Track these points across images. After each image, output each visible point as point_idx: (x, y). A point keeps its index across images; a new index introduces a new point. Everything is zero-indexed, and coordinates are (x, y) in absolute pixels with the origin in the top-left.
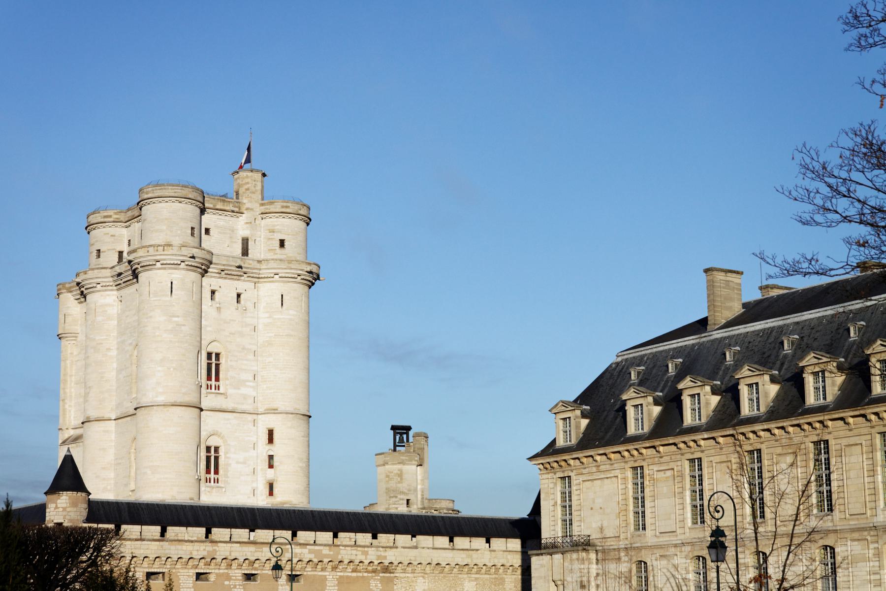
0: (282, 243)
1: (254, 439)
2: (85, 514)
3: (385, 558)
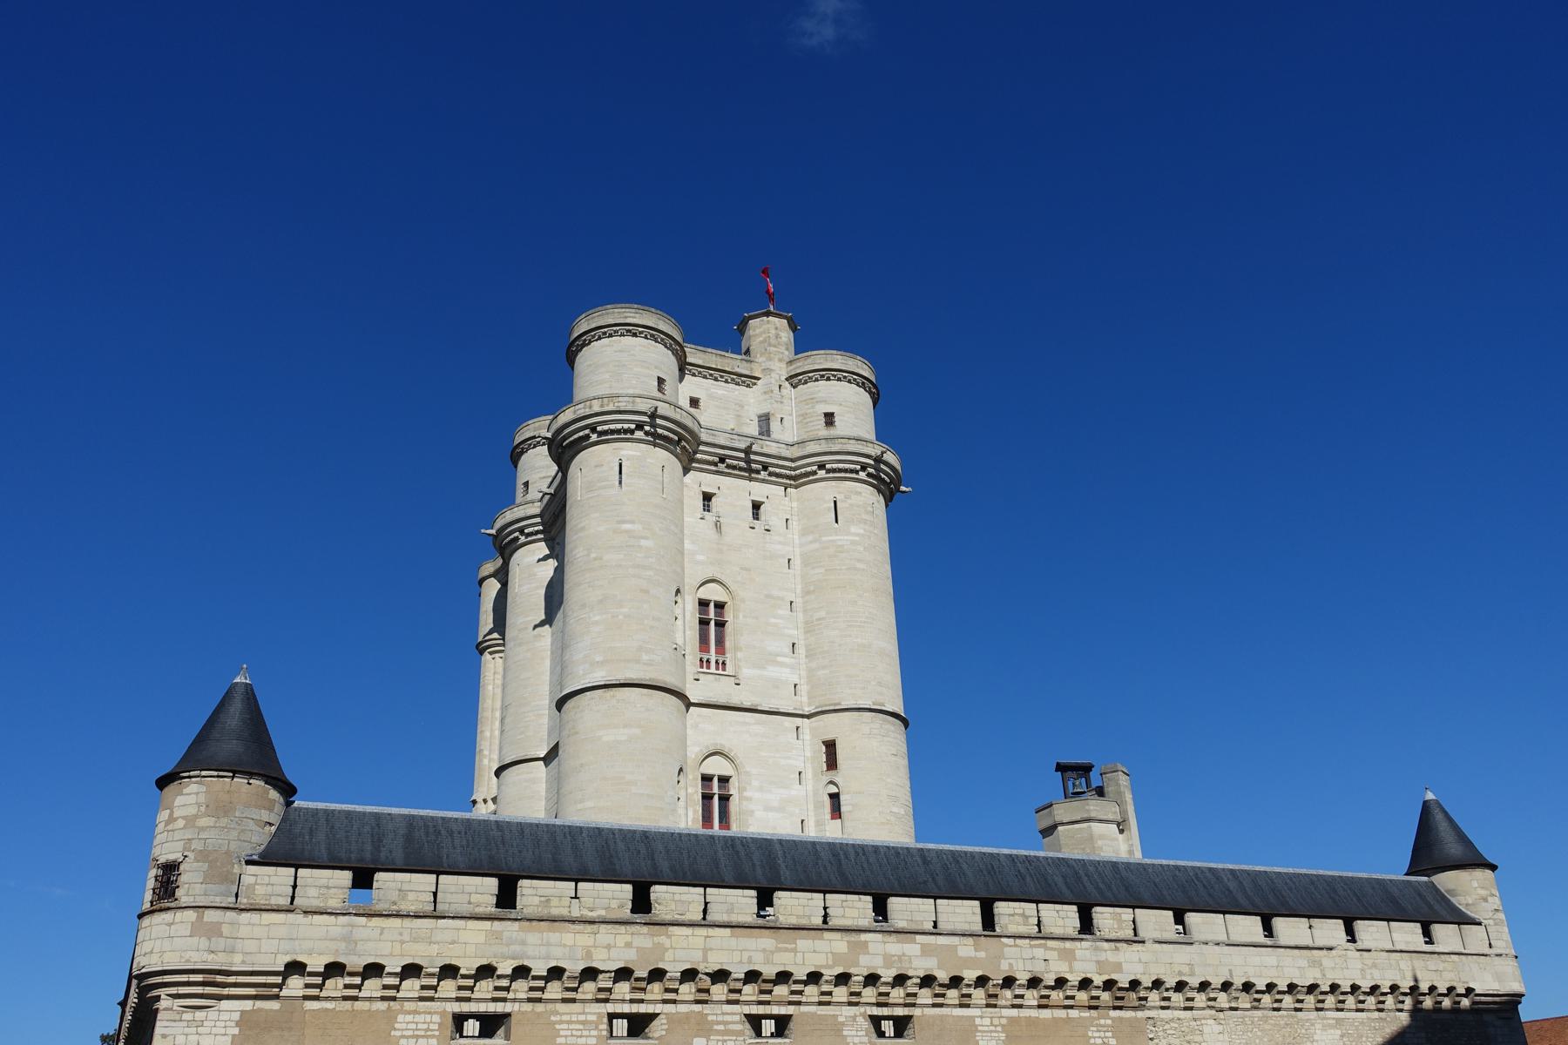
0: (829, 418)
2: (260, 838)
3: (1118, 967)
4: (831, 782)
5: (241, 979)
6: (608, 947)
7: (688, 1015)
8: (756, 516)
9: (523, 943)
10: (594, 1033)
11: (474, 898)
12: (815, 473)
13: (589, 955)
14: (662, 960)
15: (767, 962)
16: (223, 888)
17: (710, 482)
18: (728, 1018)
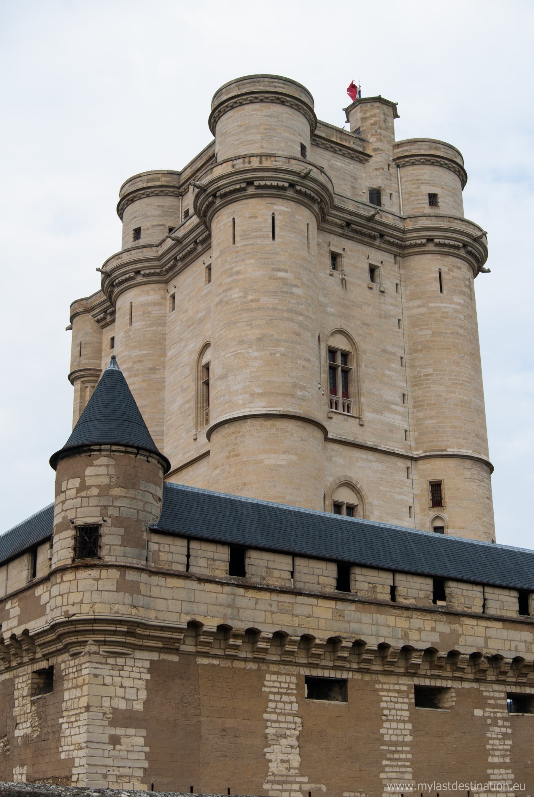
0: (433, 199)
1: (409, 500)
2: (155, 510)
4: (437, 517)
5: (154, 633)
6: (419, 630)
7: (469, 690)
8: (372, 278)
9: (360, 622)
10: (406, 700)
11: (322, 580)
12: (423, 245)
13: (406, 636)
14: (458, 644)
15: (528, 651)
16: (136, 551)
17: (338, 244)
18: (497, 695)
